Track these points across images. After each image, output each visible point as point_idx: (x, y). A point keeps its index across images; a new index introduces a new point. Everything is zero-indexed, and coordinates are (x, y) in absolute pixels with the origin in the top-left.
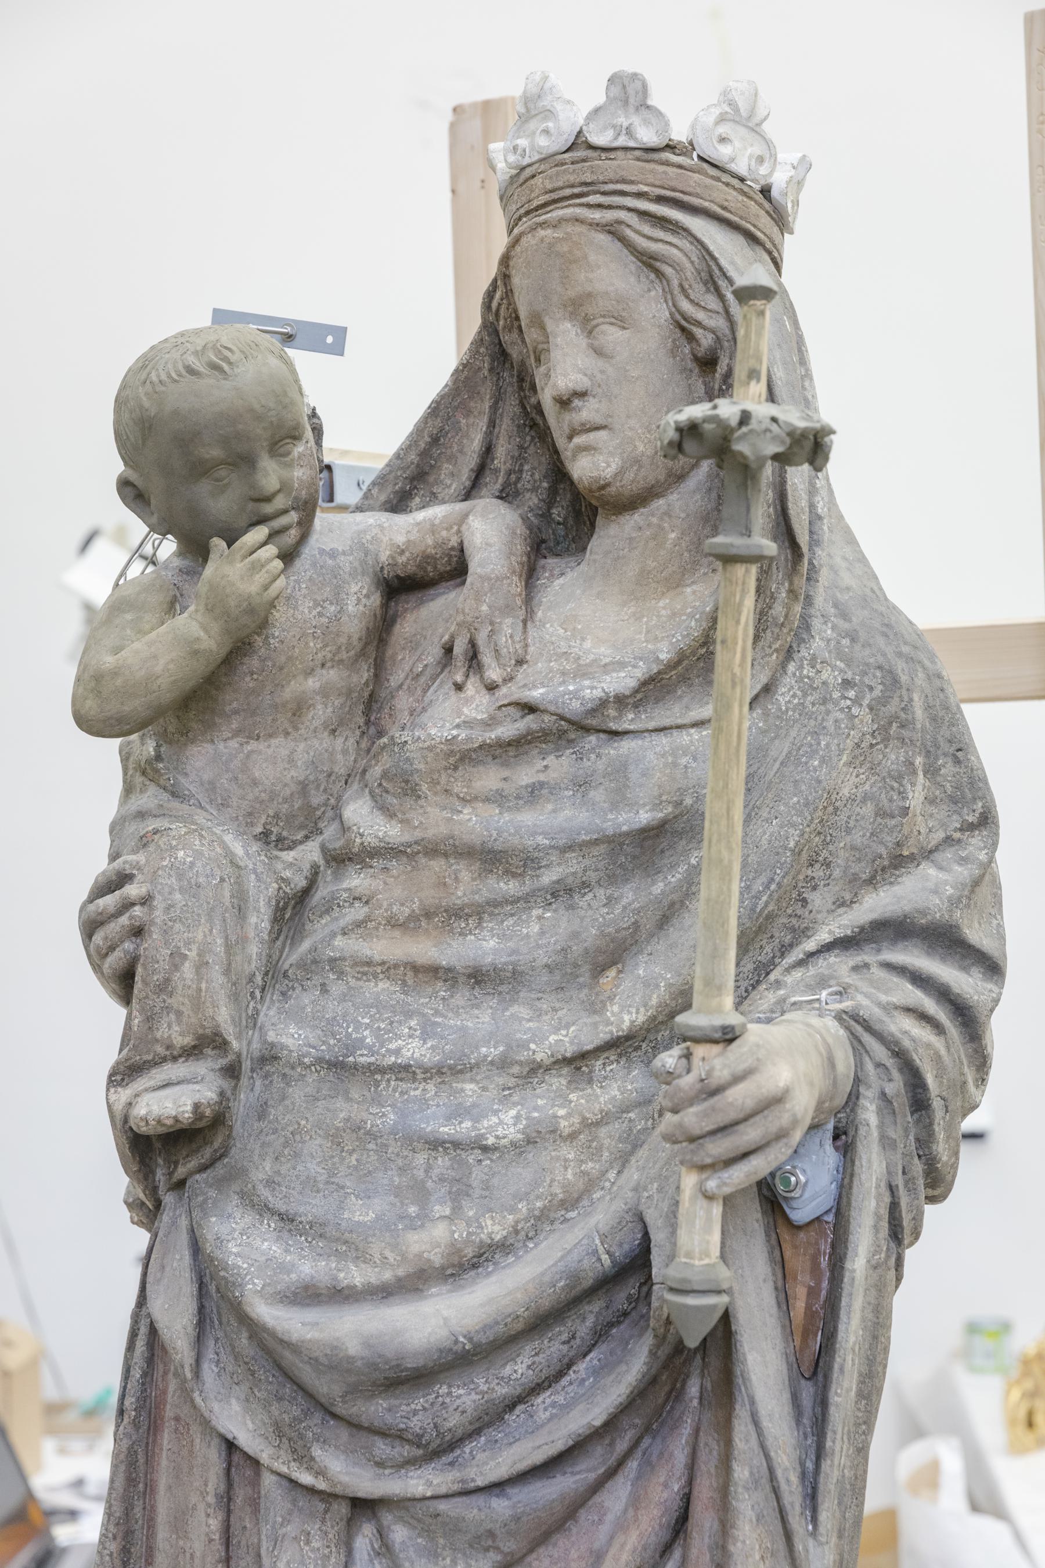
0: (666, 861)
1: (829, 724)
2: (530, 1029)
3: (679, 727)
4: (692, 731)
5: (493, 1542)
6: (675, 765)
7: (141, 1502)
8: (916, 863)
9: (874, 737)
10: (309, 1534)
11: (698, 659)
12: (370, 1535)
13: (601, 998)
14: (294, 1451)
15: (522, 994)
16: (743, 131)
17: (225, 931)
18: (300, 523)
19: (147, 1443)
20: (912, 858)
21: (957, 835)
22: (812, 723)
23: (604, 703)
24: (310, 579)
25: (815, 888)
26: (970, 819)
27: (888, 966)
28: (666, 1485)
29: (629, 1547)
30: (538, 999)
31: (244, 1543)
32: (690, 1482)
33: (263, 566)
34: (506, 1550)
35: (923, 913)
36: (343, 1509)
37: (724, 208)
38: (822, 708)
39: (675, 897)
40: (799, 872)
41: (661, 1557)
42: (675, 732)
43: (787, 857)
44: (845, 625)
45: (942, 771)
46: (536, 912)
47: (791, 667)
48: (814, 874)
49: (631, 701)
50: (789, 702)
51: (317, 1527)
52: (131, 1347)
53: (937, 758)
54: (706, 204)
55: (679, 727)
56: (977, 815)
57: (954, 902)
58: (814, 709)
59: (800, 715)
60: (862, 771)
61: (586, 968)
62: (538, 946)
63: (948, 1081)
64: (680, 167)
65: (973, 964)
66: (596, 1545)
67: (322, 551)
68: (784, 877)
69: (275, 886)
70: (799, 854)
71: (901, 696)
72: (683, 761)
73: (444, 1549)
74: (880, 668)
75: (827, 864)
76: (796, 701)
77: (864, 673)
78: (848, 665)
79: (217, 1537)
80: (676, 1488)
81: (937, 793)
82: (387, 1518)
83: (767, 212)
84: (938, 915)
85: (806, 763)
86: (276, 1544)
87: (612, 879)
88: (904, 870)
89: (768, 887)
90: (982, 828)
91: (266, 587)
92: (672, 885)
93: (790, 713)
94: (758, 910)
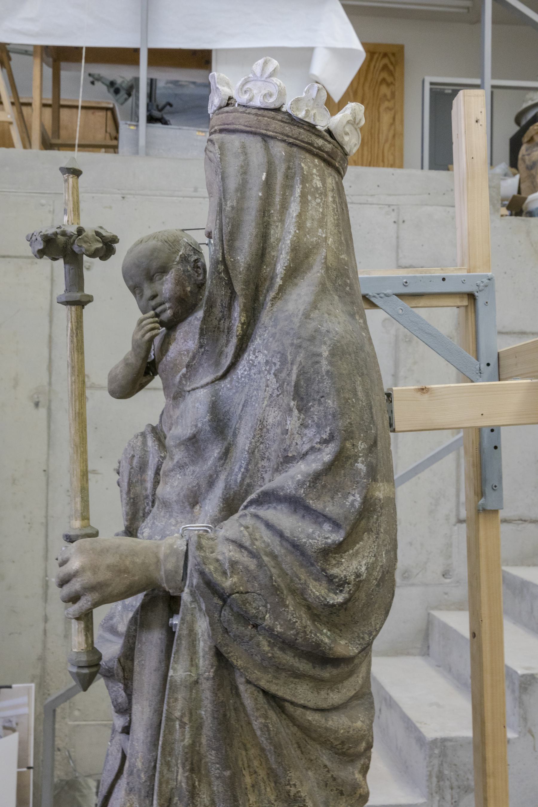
0: (207, 454)
1: (261, 384)
2: (172, 530)
3: (197, 388)
4: (202, 390)
6: (194, 407)
8: (297, 460)
9: (278, 391)
11: (202, 354)
13: (195, 519)
15: (174, 513)
16: (259, 84)
17: (130, 476)
18: (169, 308)
20: (293, 458)
21: (318, 446)
22: (255, 384)
23: (181, 378)
24: (185, 331)
25: (266, 472)
26: (324, 437)
27: (257, 516)
30: (178, 516)
33: (143, 327)
35: (282, 488)
37: (246, 126)
38: (259, 376)
39: (210, 472)
40: (257, 463)
42: (197, 391)
43: (246, 455)
44: (274, 330)
45: (312, 409)
46: (178, 476)
47: (246, 356)
48: (265, 465)
49: (187, 376)
50: (243, 374)
53: (308, 402)
54: (237, 127)
55: (197, 388)
56: (328, 435)
57: (300, 484)
58: (255, 377)
59: (248, 380)
60: (276, 409)
61: (186, 504)
62: (174, 492)
63: (260, 584)
64: (227, 112)
65: (325, 521)
67: (196, 317)
68: (247, 465)
69: (157, 459)
70: (253, 452)
71: (287, 368)
72: (197, 405)
74: (279, 352)
75: (269, 459)
76: (246, 373)
77: (273, 356)
78: (269, 352)
81: (310, 422)
83: (282, 121)
84: (288, 491)
85: (255, 405)
87: (193, 462)
88: (291, 464)
89: (240, 470)
90: (332, 442)
91: (143, 336)
92: (209, 466)
93: (243, 379)
94: (239, 482)
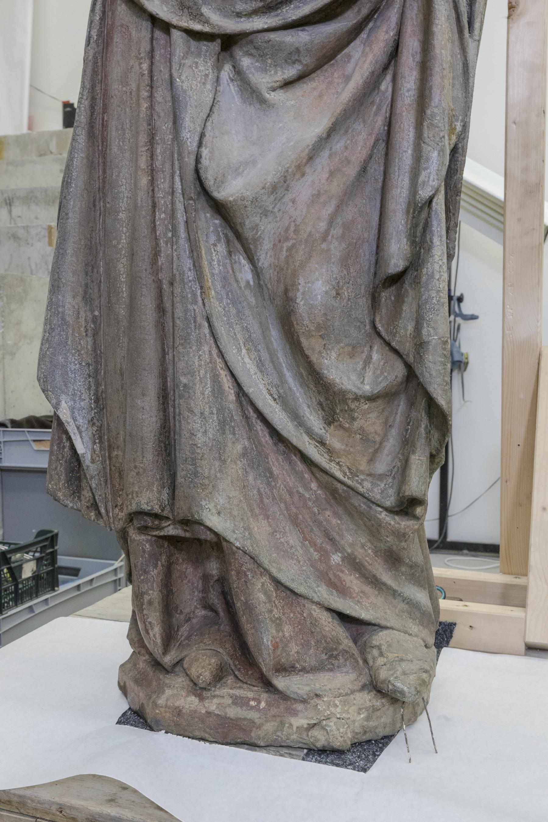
5: (299, 56)
7: (100, 85)
10: (197, 63)
12: (228, 70)
14: (190, 14)
19: (102, 57)
28: (387, 32)
29: (368, 61)
31: (160, 79)
32: (399, 33)
34: (305, 62)
36: (216, 46)
41: (383, 71)
51: (202, 59)
52: (93, 10)
66: (346, 73)
73: (270, 67)
79: (146, 72)
80: (392, 34)
82: (238, 53)
86: (180, 67)
